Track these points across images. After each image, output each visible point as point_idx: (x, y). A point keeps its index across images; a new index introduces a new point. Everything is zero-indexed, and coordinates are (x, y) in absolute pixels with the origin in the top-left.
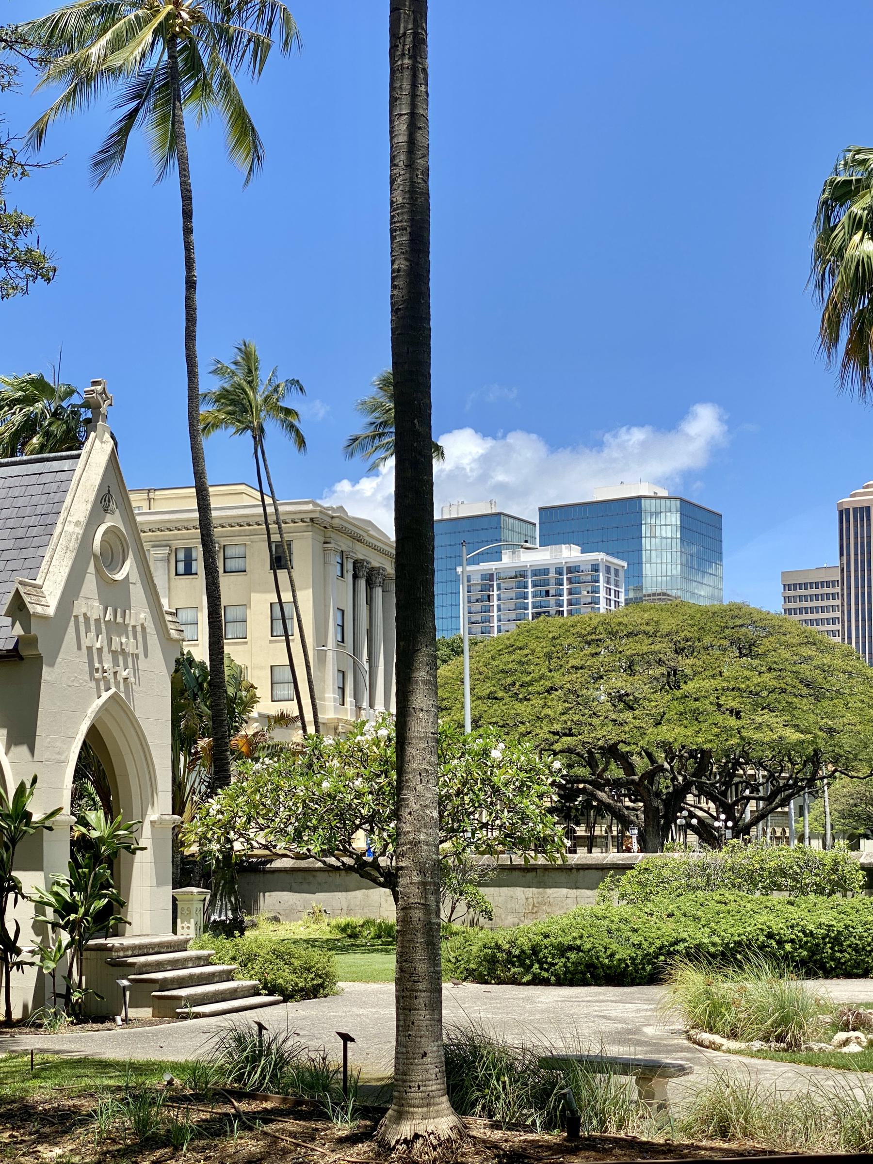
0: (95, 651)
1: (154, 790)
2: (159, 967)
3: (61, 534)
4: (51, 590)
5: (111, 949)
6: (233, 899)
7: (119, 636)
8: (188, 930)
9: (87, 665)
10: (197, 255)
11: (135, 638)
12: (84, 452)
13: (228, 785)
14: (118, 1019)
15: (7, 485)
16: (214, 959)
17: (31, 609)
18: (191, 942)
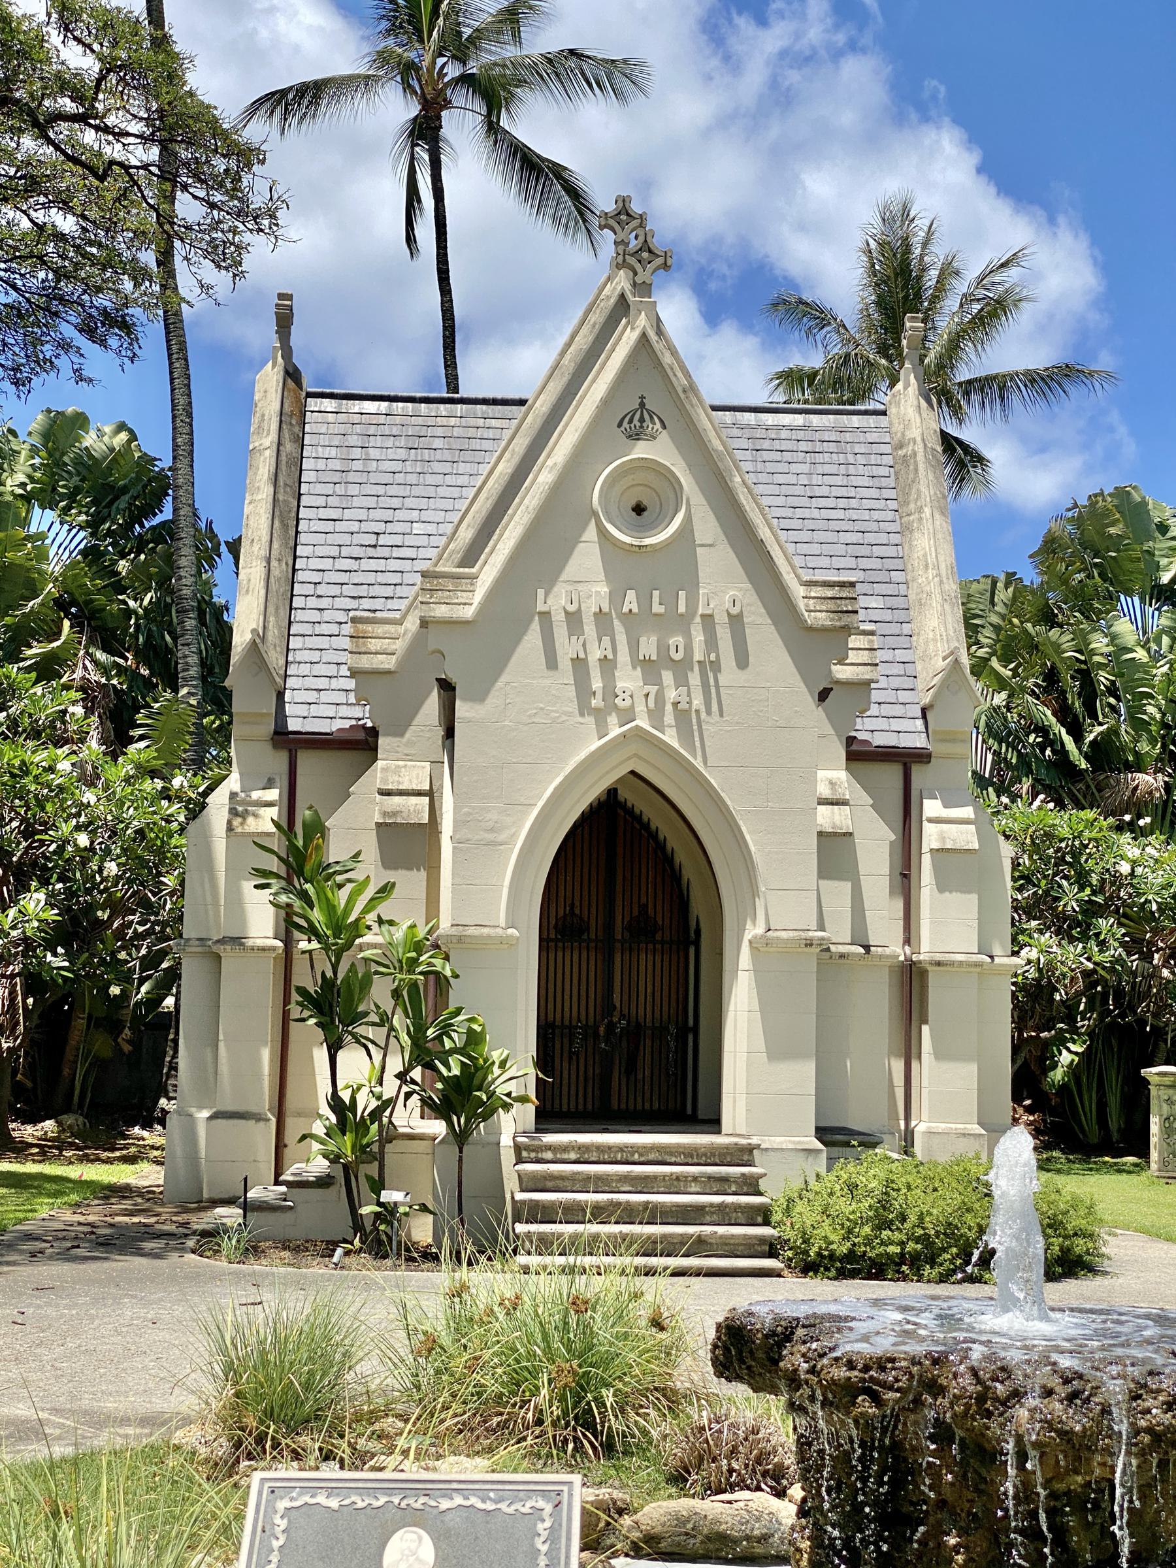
9: (573, 688)
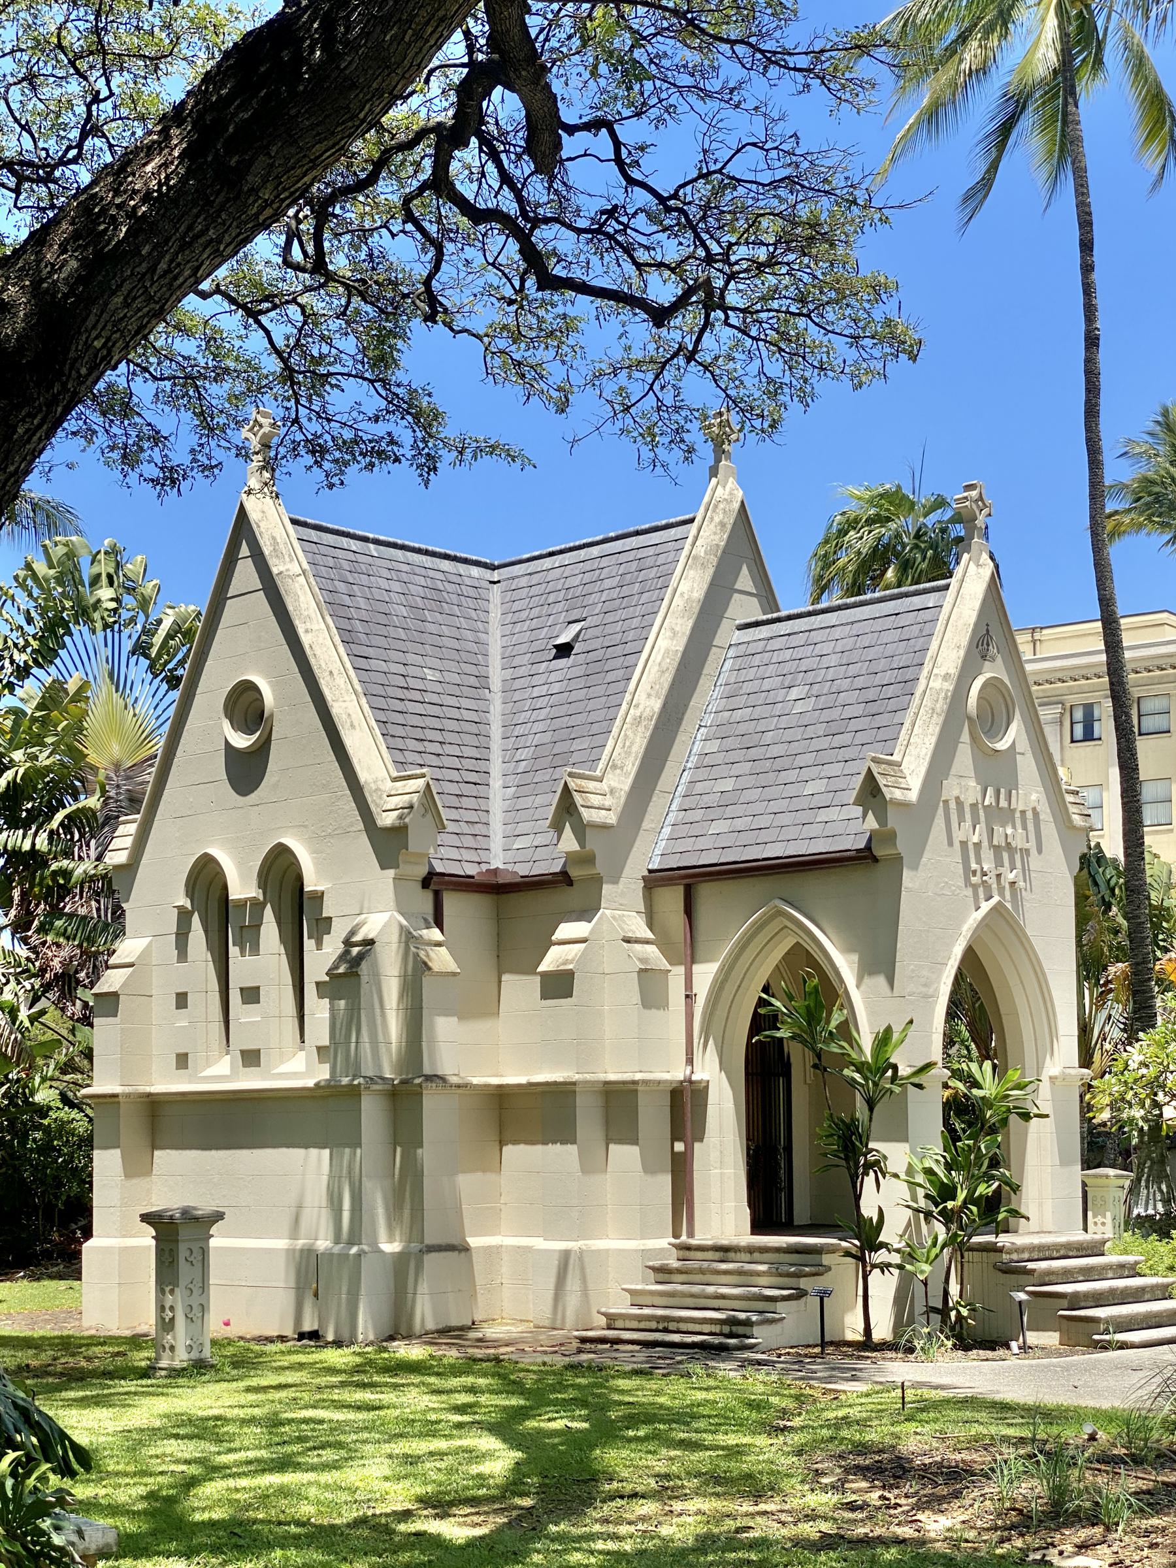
0: (971, 847)
1: (1053, 1034)
2: (1068, 1276)
3: (925, 692)
4: (912, 768)
5: (1000, 1250)
6: (1164, 1187)
7: (1003, 826)
8: (1103, 1227)
9: (961, 866)
10: (1100, 301)
11: (1025, 828)
12: (954, 582)
13: (1153, 1026)
14: (1014, 1345)
15: (855, 633)
16: (1142, 1268)
17: (888, 793)
18: (1108, 1245)
